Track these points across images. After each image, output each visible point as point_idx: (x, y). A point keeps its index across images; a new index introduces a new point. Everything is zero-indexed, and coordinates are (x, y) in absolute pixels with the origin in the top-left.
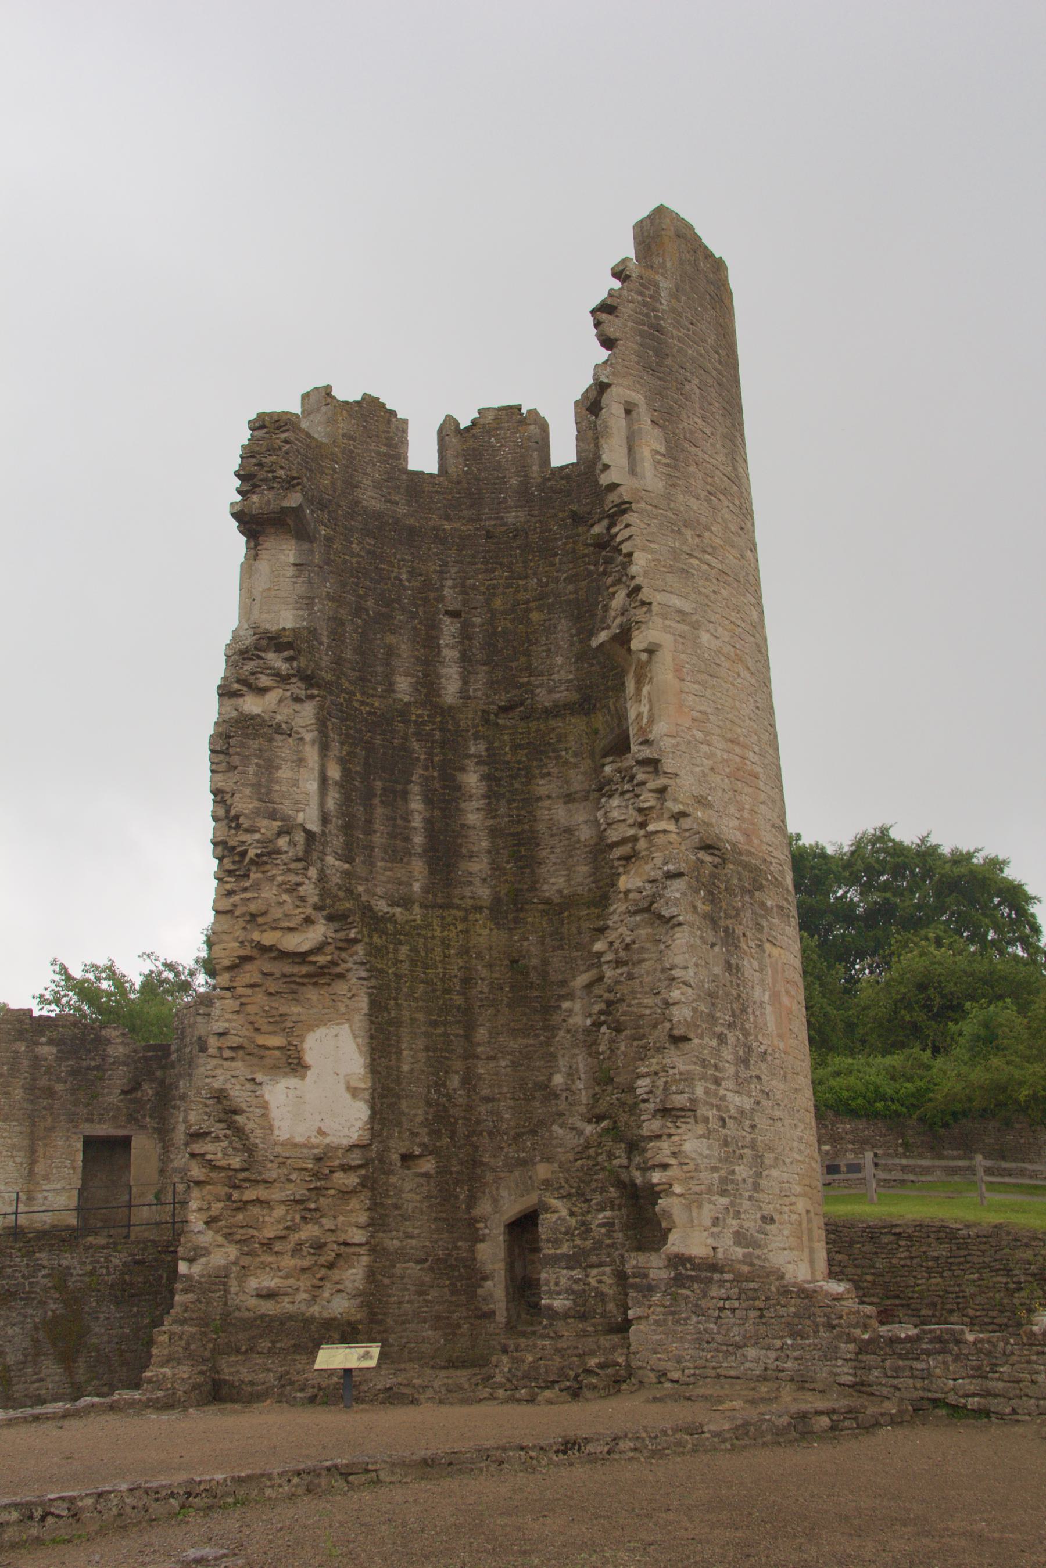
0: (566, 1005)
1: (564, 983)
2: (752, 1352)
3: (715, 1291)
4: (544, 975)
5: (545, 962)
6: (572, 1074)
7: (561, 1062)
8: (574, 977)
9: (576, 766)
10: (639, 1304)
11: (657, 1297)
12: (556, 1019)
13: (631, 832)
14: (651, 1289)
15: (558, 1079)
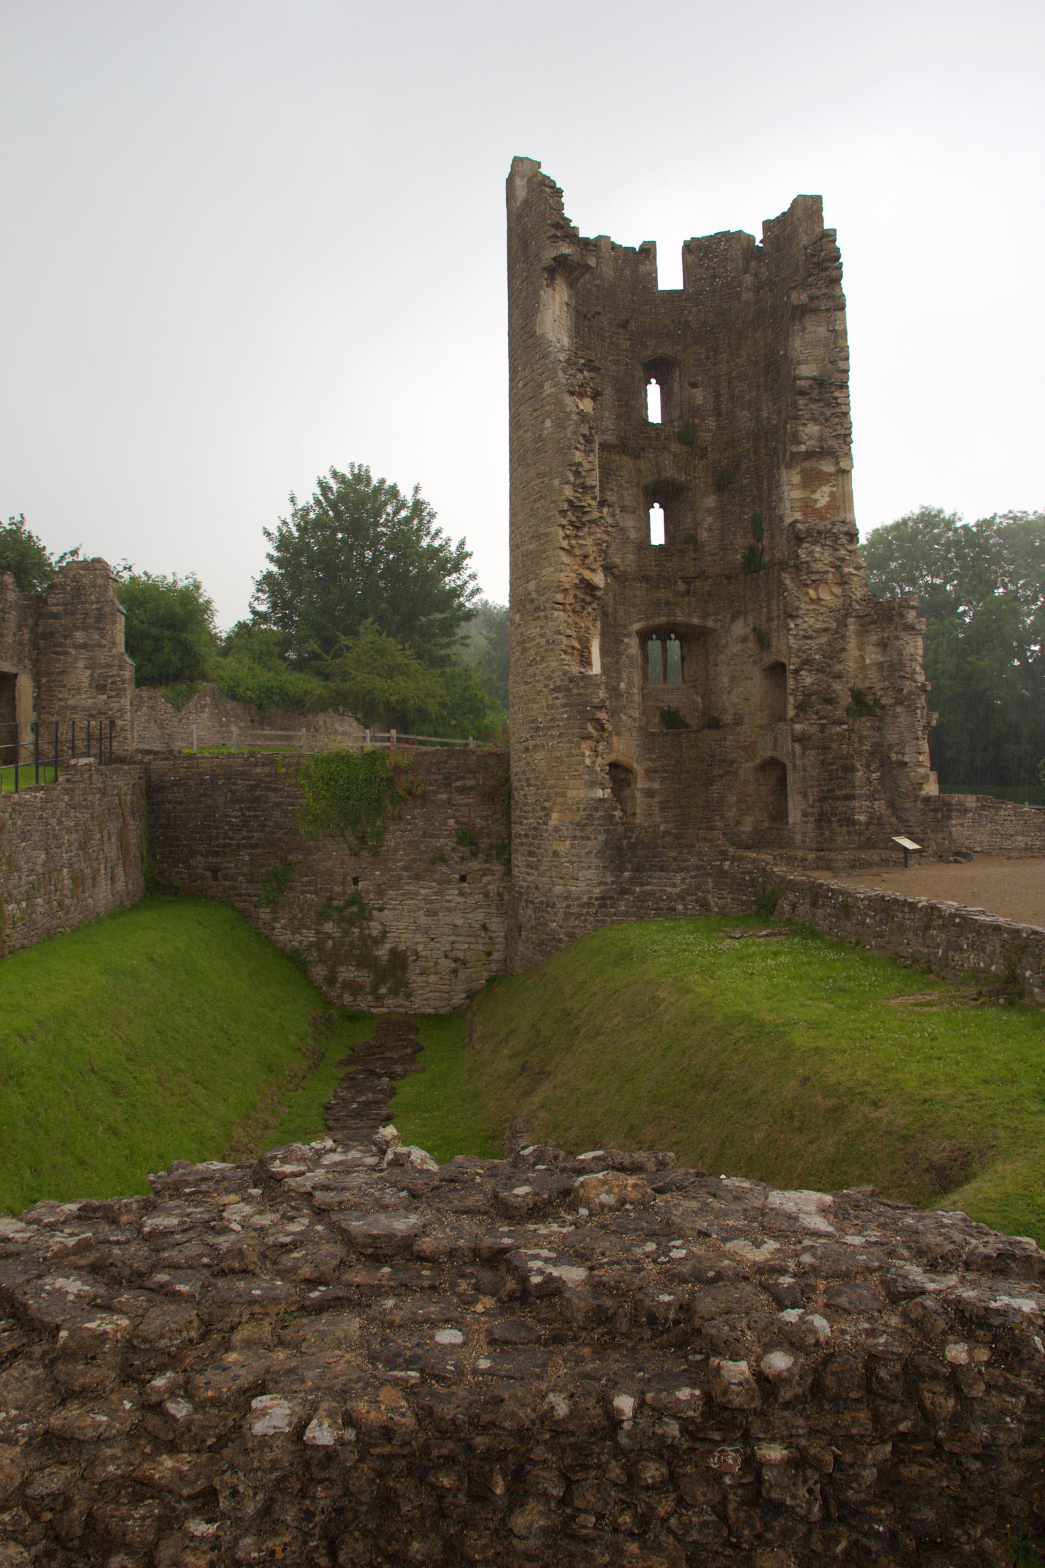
0: (626, 640)
1: (625, 627)
2: (1020, 838)
3: (1002, 813)
4: (615, 620)
5: (616, 612)
6: (630, 684)
7: (624, 676)
8: (631, 624)
9: (627, 489)
10: (958, 817)
11: (969, 815)
12: (622, 648)
13: (828, 568)
14: (966, 811)
15: (623, 686)
